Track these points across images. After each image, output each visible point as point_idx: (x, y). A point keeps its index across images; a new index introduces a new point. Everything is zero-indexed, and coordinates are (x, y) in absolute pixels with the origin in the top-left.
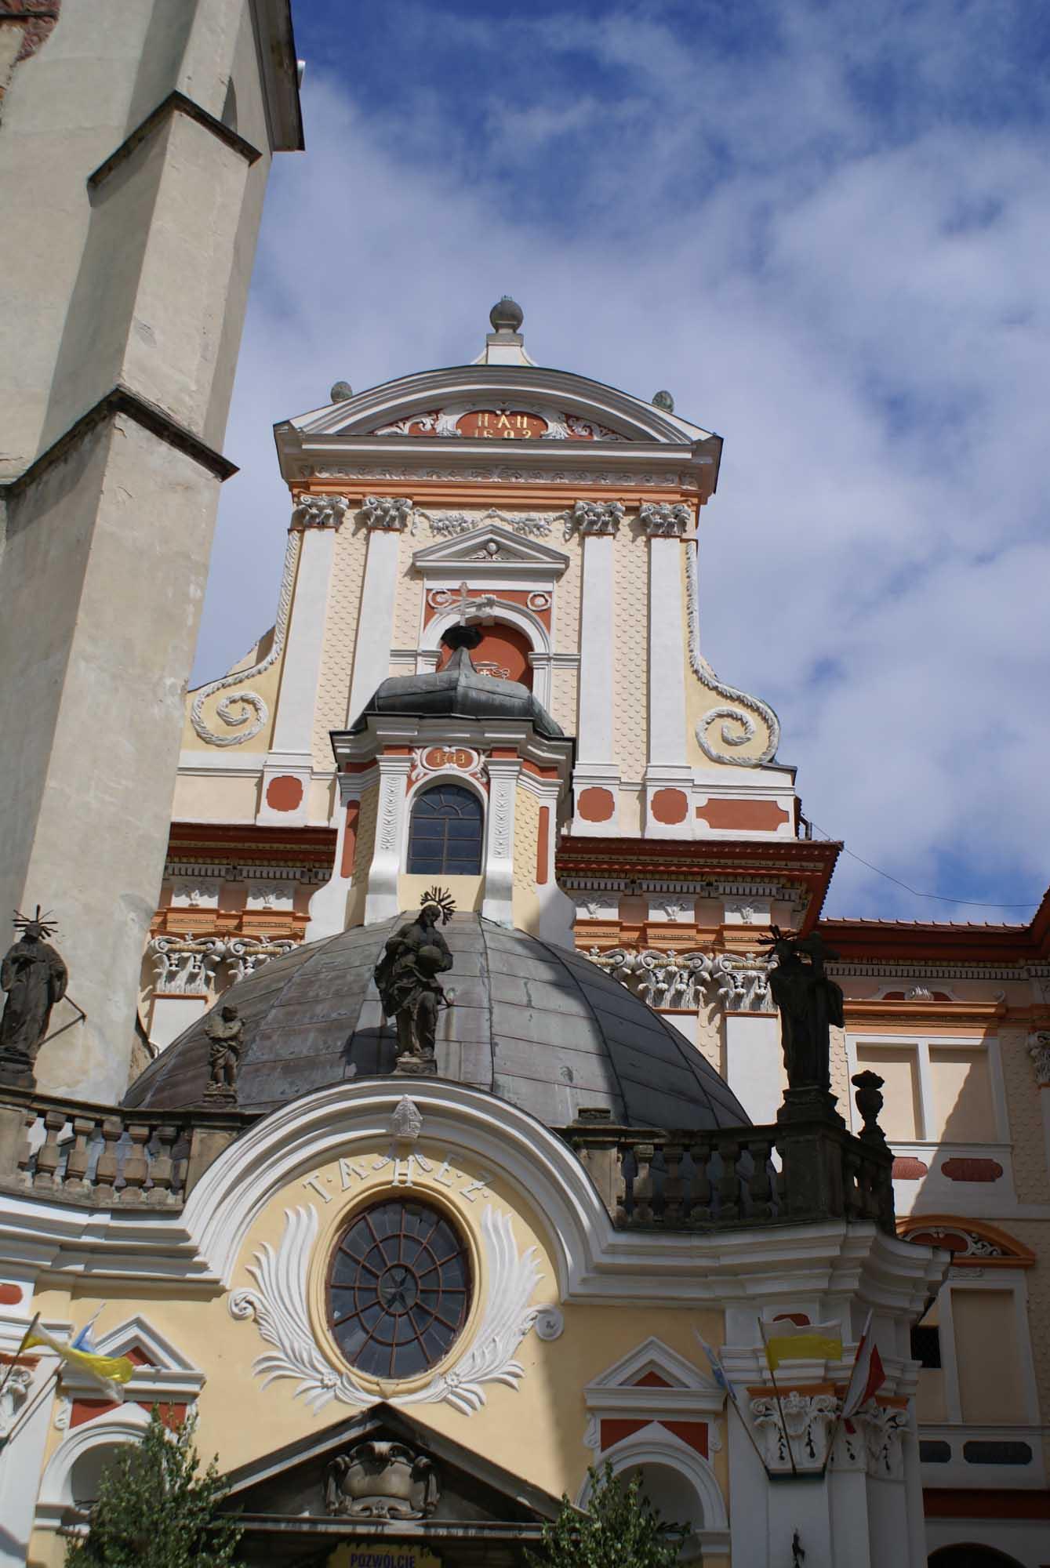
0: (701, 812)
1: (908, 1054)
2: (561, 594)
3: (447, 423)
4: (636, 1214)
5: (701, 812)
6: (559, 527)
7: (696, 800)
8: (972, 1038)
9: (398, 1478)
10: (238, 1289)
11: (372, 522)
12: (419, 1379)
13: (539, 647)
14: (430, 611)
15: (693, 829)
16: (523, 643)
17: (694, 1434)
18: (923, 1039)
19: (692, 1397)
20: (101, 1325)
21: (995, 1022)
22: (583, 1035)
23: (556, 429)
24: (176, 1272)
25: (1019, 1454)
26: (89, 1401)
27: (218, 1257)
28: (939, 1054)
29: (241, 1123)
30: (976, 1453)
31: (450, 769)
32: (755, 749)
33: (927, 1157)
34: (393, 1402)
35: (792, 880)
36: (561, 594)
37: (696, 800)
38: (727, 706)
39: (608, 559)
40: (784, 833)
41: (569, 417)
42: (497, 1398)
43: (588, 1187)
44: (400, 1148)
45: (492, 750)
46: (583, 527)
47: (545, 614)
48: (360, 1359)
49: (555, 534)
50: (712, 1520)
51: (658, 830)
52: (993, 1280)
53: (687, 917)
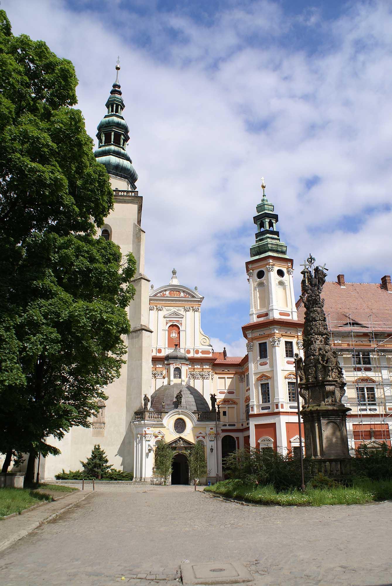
1: (224, 378)
2: (183, 320)
3: (167, 292)
4: (199, 420)
6: (183, 310)
7: (200, 351)
8: (232, 376)
9: (181, 442)
10: (167, 427)
11: (159, 310)
13: (181, 329)
14: (167, 323)
15: (200, 355)
16: (179, 329)
17: (204, 437)
18: (226, 376)
19: (204, 435)
20: (156, 430)
21: (235, 374)
22: (194, 400)
23: (182, 294)
24: (162, 426)
25: (234, 425)
26: (156, 437)
27: (165, 425)
28: (228, 378)
29: (167, 413)
30: (230, 425)
31: (178, 366)
32: (207, 344)
33: (226, 391)
36: (183, 320)
37: (200, 351)
39: (190, 314)
40: (210, 355)
41: (184, 292)
42: (189, 435)
43: (195, 417)
44: (179, 414)
45: (182, 364)
46: (186, 310)
47: (181, 324)
49: (182, 312)
50: (205, 444)
51: (196, 356)
53: (199, 367)
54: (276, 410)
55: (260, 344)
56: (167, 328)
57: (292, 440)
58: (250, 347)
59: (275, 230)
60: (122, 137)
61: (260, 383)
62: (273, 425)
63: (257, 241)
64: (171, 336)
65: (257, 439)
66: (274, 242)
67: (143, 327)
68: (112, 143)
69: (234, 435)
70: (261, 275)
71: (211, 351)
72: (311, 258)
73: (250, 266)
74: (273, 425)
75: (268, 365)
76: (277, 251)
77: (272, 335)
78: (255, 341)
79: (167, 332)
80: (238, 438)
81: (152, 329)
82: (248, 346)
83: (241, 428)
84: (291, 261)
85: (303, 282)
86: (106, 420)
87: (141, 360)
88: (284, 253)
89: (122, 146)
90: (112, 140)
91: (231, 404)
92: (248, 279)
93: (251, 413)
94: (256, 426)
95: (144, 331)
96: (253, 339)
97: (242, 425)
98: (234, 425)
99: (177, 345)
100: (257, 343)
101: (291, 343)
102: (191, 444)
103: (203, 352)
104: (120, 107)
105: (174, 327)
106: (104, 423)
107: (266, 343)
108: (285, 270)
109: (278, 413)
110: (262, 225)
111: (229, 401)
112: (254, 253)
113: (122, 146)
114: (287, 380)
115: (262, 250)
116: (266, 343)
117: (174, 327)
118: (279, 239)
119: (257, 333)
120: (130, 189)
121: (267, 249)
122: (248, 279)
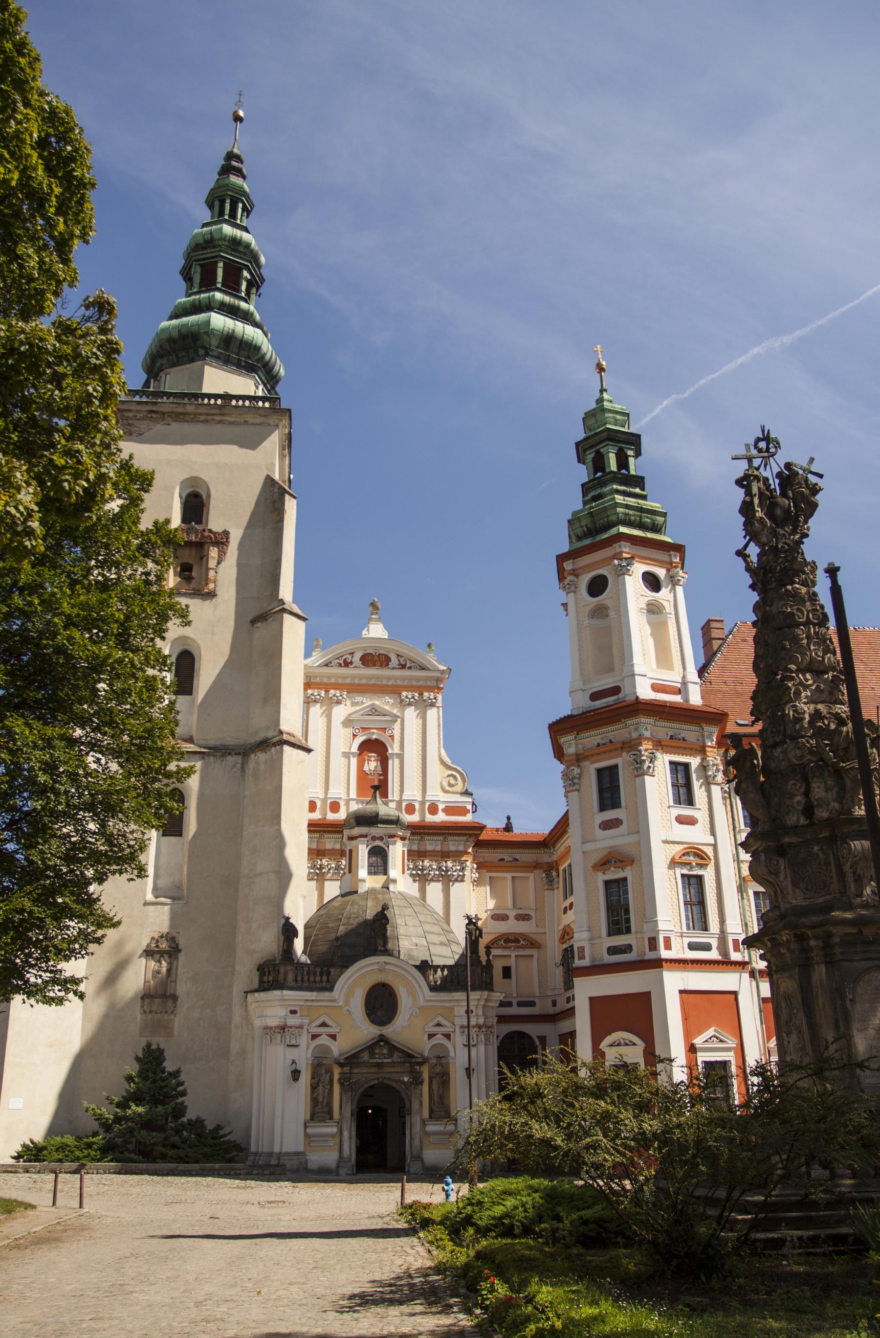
0: (443, 810)
5: (443, 810)
7: (441, 806)
12: (387, 1026)
14: (355, 736)
15: (441, 817)
25: (532, 1004)
30: (520, 1004)
32: (459, 787)
34: (383, 1032)
35: (471, 835)
38: (450, 772)
40: (468, 818)
44: (380, 971)
46: (404, 704)
47: (392, 737)
48: (373, 1021)
51: (430, 818)
52: (528, 952)
54: (650, 955)
55: (599, 771)
56: (355, 749)
57: (698, 1041)
58: (571, 783)
59: (633, 472)
60: (246, 274)
61: (601, 878)
62: (645, 997)
63: (585, 503)
64: (366, 768)
65: (596, 1039)
66: (631, 501)
67: (285, 737)
68: (219, 286)
69: (533, 1030)
70: (598, 586)
71: (469, 807)
72: (767, 438)
73: (568, 566)
74: (645, 997)
75: (623, 828)
76: (641, 526)
77: (631, 746)
78: (586, 764)
79: (354, 761)
80: (543, 1039)
81: (310, 745)
82: (566, 776)
83: (551, 1010)
84: (679, 548)
85: (746, 509)
86: (182, 989)
87: (279, 823)
88: (656, 529)
89: (243, 295)
90: (220, 279)
91: (524, 947)
92: (565, 605)
93: (577, 963)
94: (595, 1002)
95: (286, 748)
96: (579, 759)
97: (554, 1003)
98: (532, 1004)
99: (380, 788)
100: (591, 768)
101: (686, 766)
102: (413, 1057)
103: (448, 810)
104: (240, 205)
105: (374, 747)
106: (174, 998)
107: (616, 766)
108: (661, 573)
109: (658, 963)
110: (599, 463)
111: (517, 941)
112: (579, 531)
113: (243, 295)
114: (679, 871)
115: (600, 523)
116: (616, 766)
117: (374, 747)
118: (644, 497)
119: (592, 739)
120: (260, 393)
121: (613, 518)
122: (565, 605)
